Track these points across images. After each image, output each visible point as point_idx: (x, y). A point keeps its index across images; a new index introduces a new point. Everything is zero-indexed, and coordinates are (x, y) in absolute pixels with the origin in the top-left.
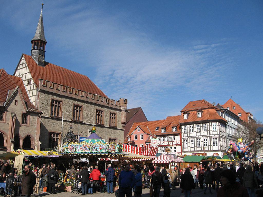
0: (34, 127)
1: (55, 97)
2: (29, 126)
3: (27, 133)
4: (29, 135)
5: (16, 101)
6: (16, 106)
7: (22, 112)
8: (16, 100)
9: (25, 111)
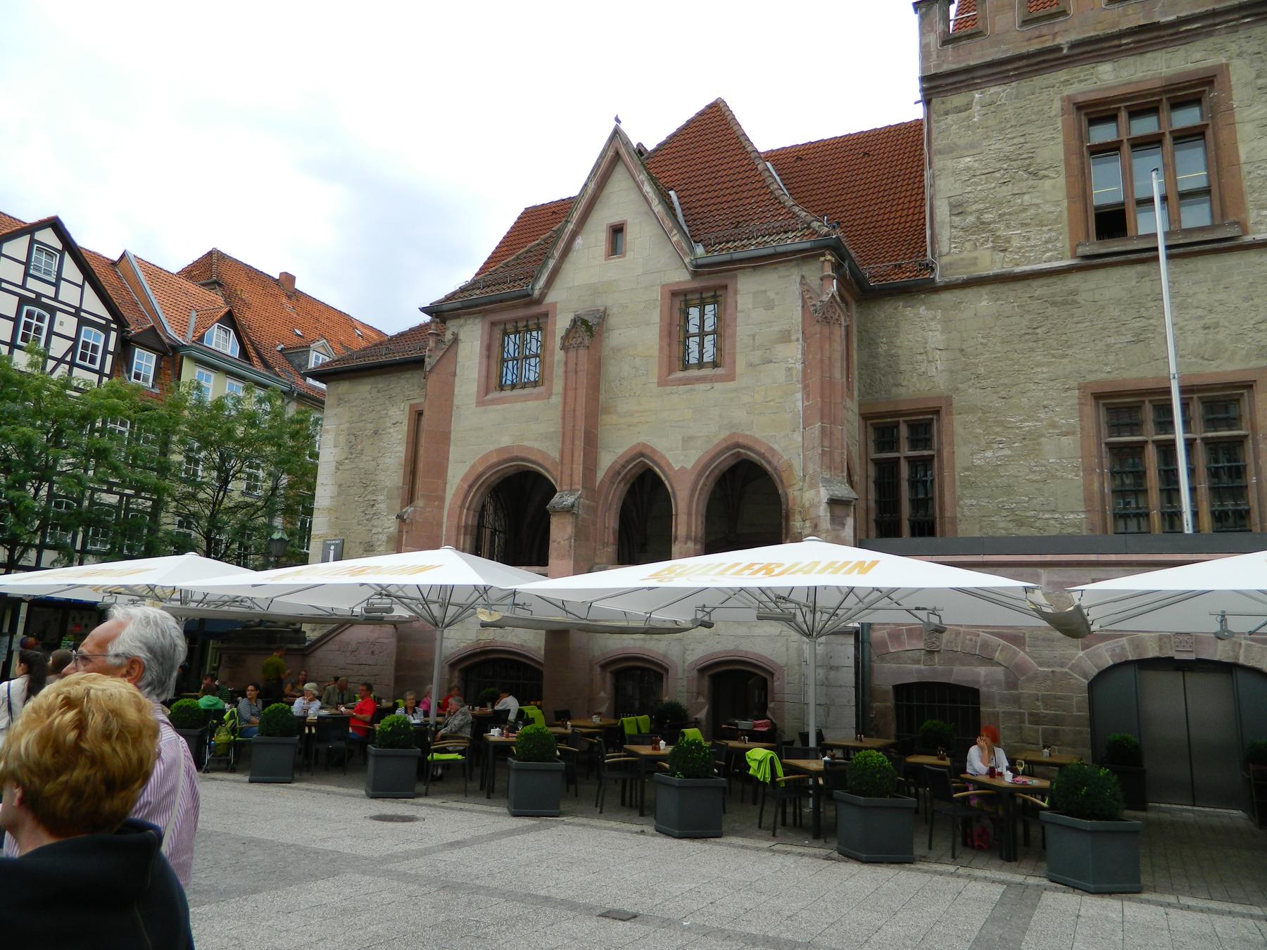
0: (781, 376)
1: (1108, 77)
2: (731, 377)
3: (724, 434)
4: (738, 445)
5: (617, 231)
6: (616, 261)
7: (663, 286)
8: (615, 220)
9: (680, 276)
